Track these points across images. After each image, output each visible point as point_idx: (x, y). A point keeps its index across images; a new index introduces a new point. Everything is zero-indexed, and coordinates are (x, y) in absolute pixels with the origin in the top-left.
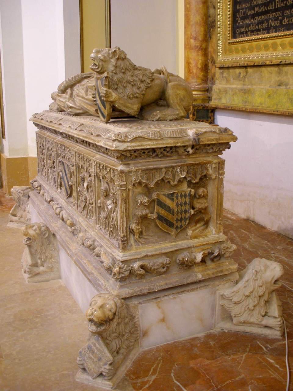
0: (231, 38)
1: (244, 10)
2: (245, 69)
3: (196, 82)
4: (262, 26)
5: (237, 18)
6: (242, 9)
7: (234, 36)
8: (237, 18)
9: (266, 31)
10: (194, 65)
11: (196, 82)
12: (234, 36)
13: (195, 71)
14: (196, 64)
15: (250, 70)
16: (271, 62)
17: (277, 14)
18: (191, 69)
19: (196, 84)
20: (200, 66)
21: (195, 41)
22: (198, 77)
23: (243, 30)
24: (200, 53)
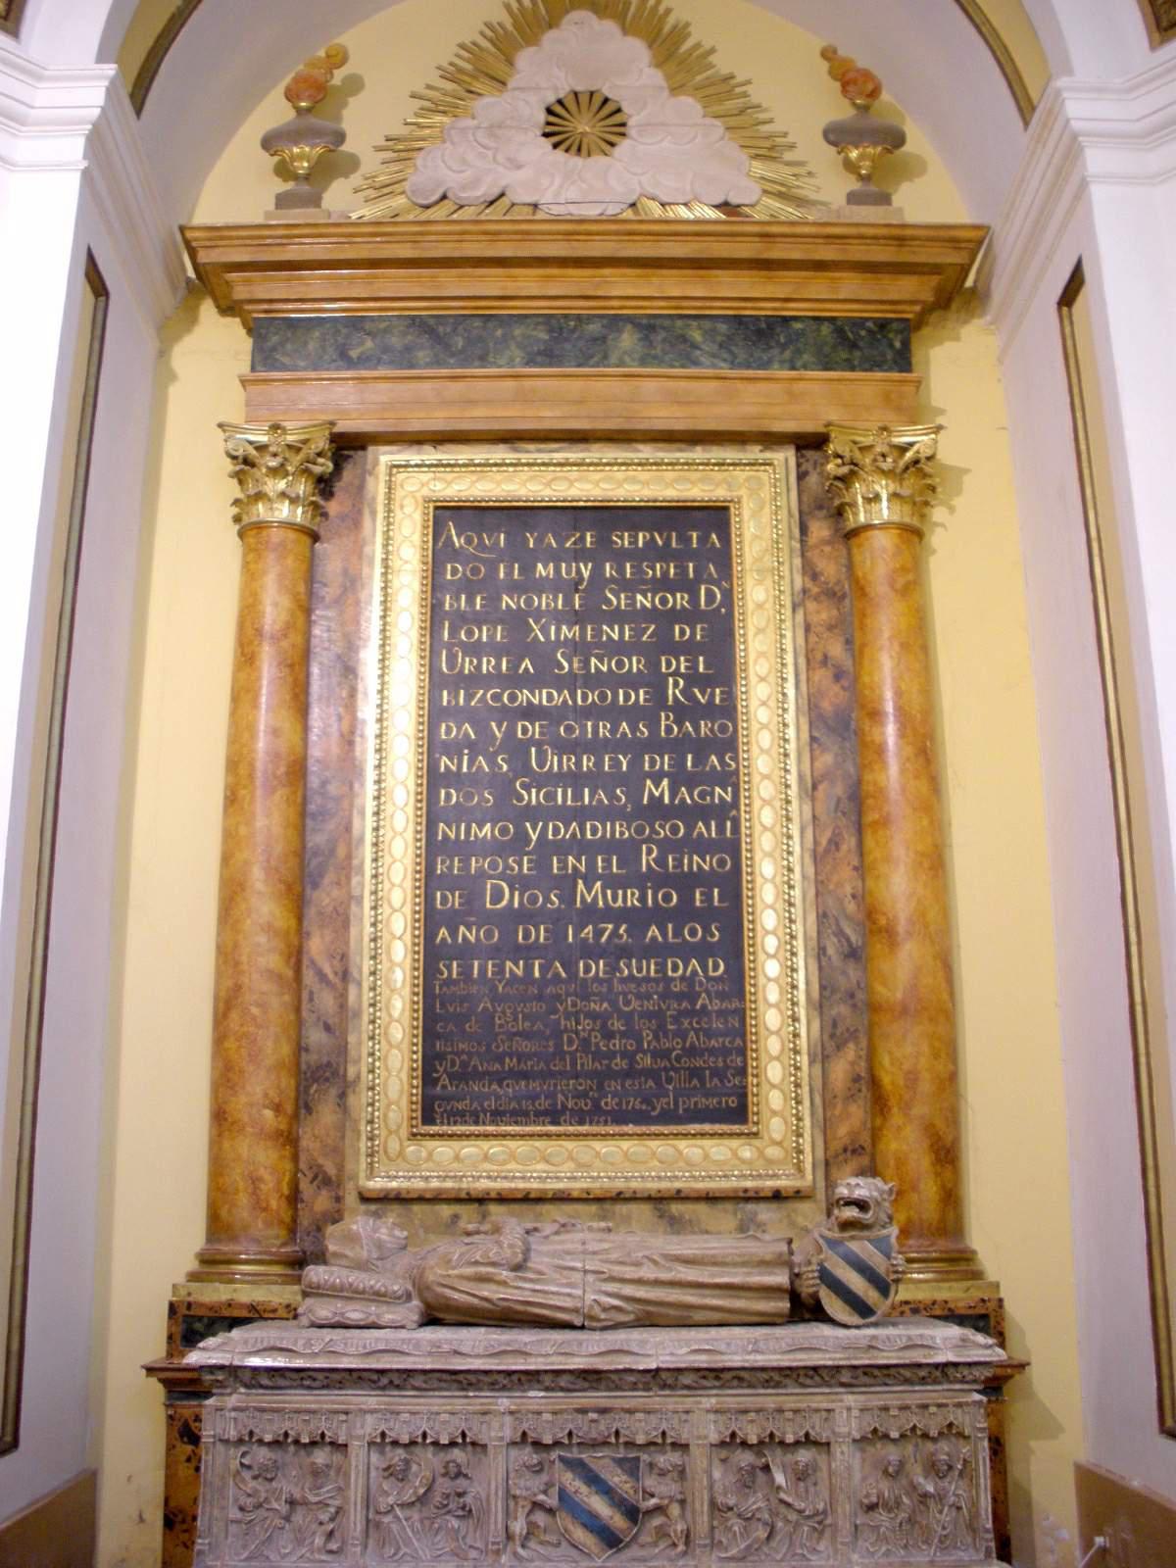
0: (420, 1120)
1: (464, 1057)
2: (476, 1205)
3: (277, 1237)
4: (534, 1105)
5: (437, 1071)
6: (458, 1054)
7: (428, 1118)
8: (437, 1071)
9: (548, 1120)
10: (271, 1185)
11: (277, 1237)
12: (428, 1118)
13: (274, 1204)
14: (279, 1182)
15: (493, 1208)
16: (588, 1194)
17: (581, 1085)
18: (263, 1197)
19: (278, 1242)
20: (286, 1191)
21: (277, 1117)
22: (281, 1222)
23: (460, 1106)
24: (287, 1153)
